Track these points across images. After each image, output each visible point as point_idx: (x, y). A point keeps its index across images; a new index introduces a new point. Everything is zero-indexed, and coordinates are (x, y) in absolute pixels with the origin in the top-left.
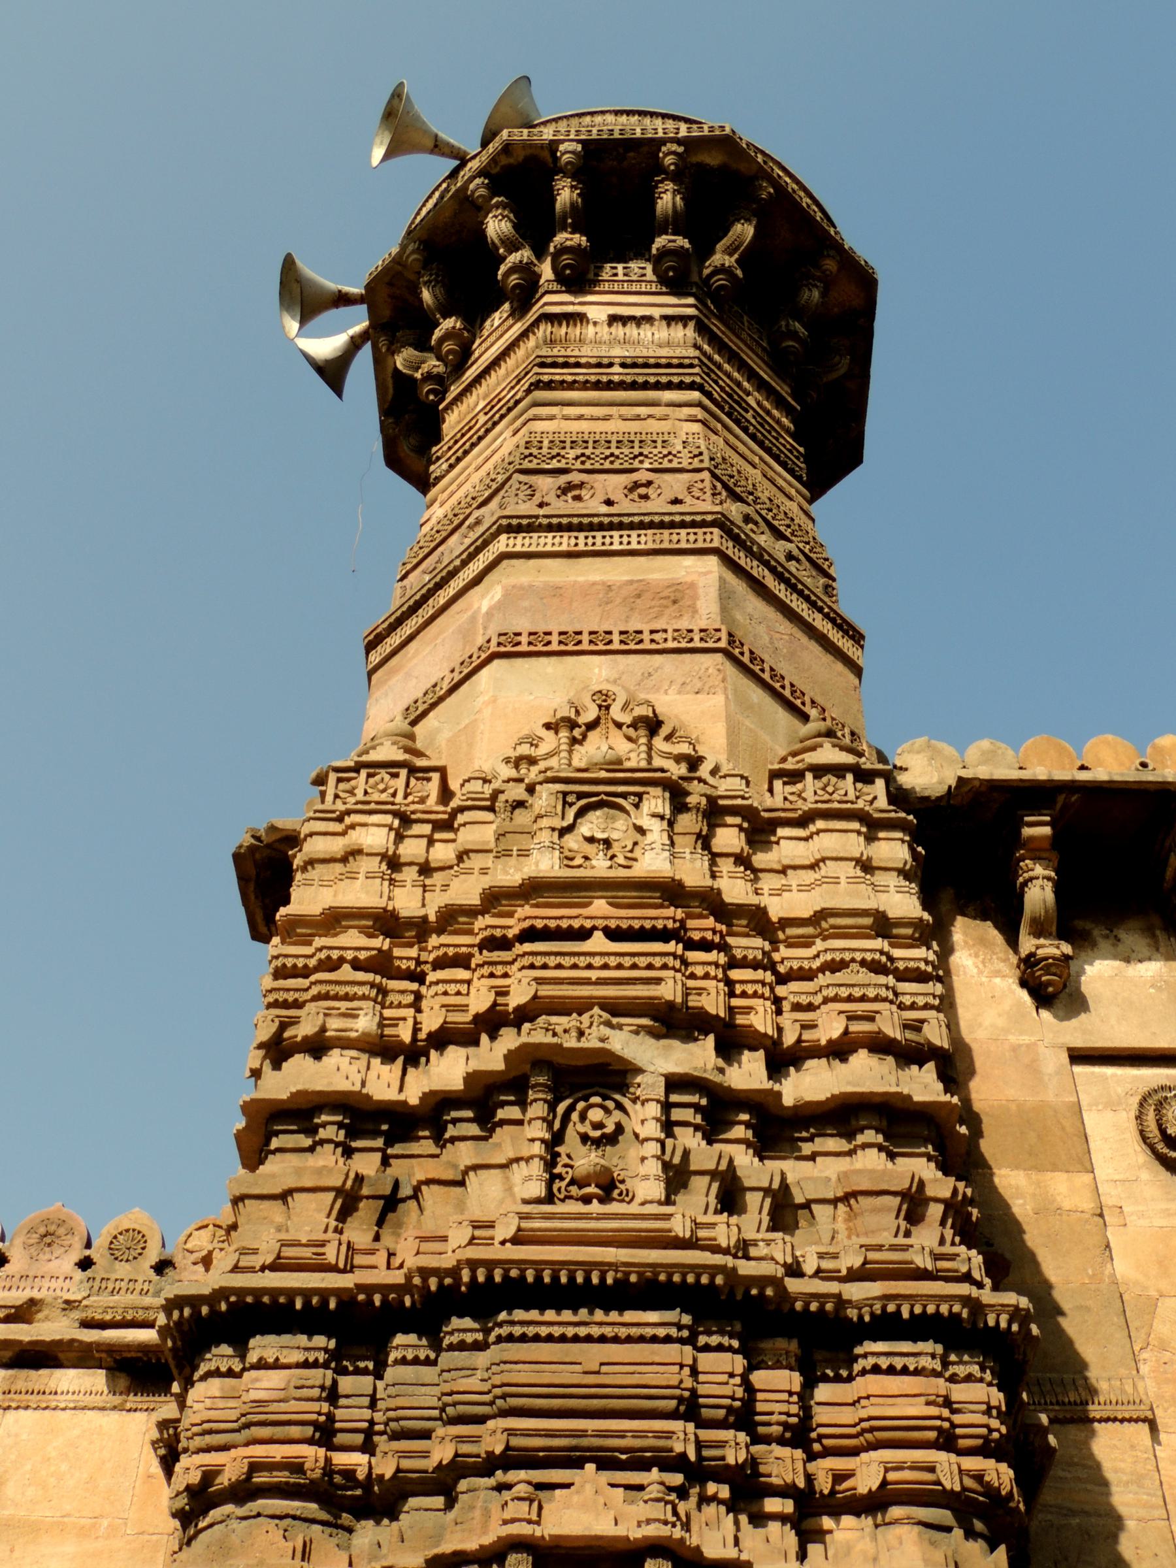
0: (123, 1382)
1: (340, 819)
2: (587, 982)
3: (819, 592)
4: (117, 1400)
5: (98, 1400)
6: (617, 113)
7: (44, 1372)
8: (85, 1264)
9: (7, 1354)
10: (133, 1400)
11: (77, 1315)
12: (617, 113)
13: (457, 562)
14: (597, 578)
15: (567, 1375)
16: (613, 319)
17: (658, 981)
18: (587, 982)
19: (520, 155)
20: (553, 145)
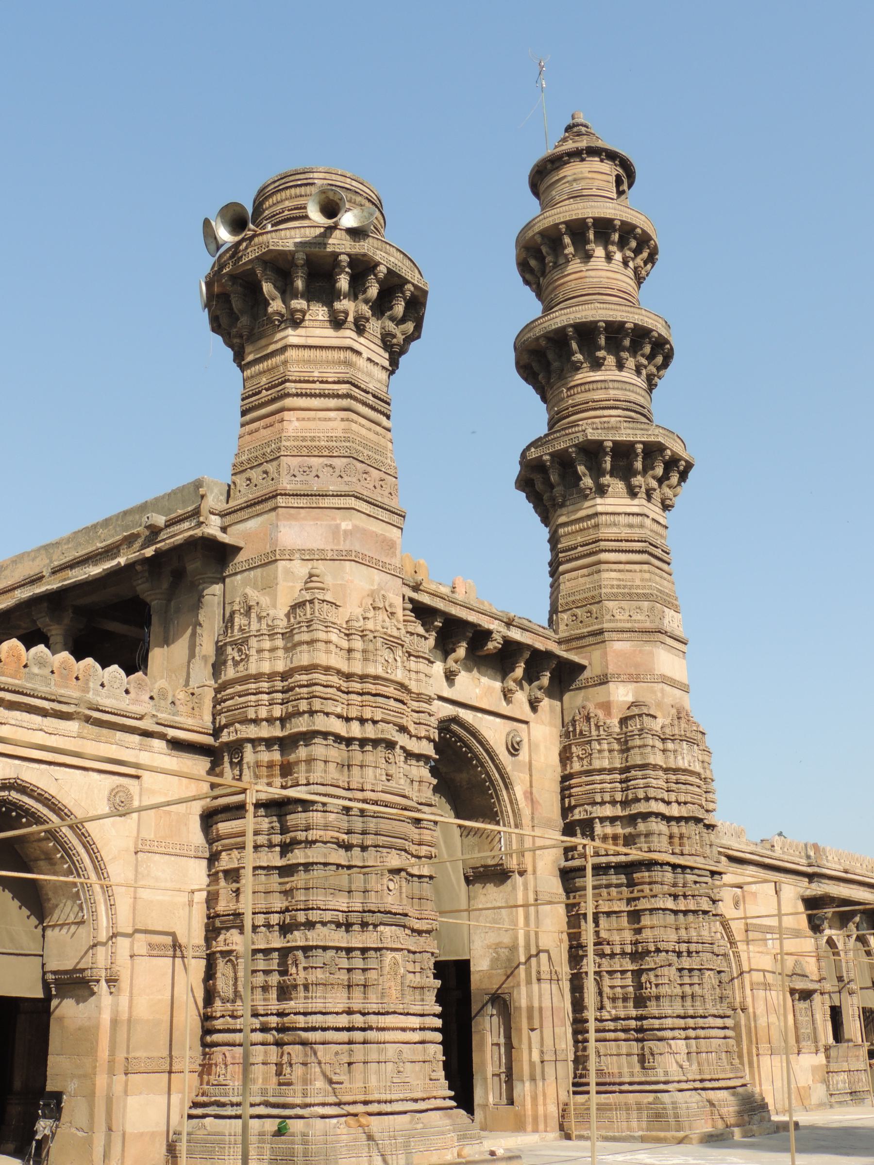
0: (170, 746)
1: (326, 627)
2: (389, 715)
3: (450, 594)
4: (169, 752)
5: (162, 751)
6: (398, 250)
7: (150, 739)
8: (152, 698)
9: (140, 732)
10: (174, 753)
11: (155, 719)
12: (398, 250)
13: (331, 493)
14: (374, 529)
15: (390, 827)
16: (369, 359)
17: (402, 718)
18: (389, 715)
19: (365, 259)
20: (378, 264)
